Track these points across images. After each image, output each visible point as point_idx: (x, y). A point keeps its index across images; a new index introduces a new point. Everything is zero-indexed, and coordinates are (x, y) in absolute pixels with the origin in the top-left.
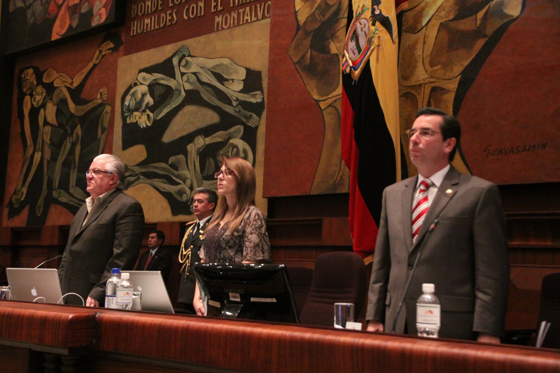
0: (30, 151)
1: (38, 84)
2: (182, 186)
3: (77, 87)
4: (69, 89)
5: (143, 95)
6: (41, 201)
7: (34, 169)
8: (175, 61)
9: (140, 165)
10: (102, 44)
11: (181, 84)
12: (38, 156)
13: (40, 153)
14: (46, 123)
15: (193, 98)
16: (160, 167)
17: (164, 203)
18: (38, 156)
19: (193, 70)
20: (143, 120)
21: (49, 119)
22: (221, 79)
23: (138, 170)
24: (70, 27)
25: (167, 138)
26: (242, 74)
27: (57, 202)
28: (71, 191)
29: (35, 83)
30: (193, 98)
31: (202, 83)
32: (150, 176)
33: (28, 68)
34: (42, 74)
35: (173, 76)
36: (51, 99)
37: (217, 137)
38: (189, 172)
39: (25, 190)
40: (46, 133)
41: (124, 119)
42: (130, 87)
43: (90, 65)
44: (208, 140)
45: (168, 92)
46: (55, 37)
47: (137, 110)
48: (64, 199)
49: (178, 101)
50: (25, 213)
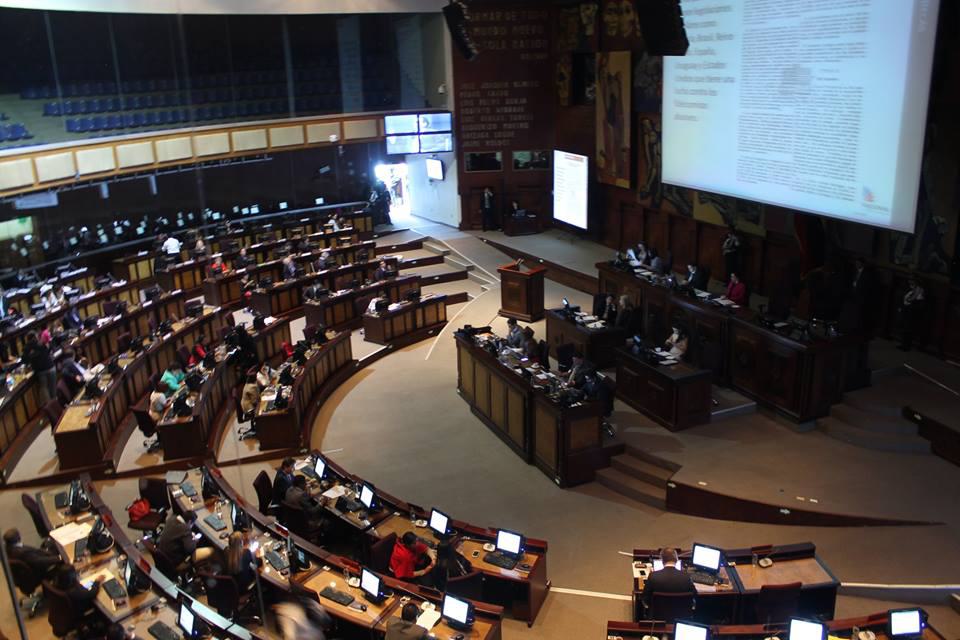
0: (650, 166)
6: (658, 195)
7: (653, 177)
17: (720, 217)
27: (666, 198)
39: (648, 187)
48: (670, 198)
50: (650, 199)
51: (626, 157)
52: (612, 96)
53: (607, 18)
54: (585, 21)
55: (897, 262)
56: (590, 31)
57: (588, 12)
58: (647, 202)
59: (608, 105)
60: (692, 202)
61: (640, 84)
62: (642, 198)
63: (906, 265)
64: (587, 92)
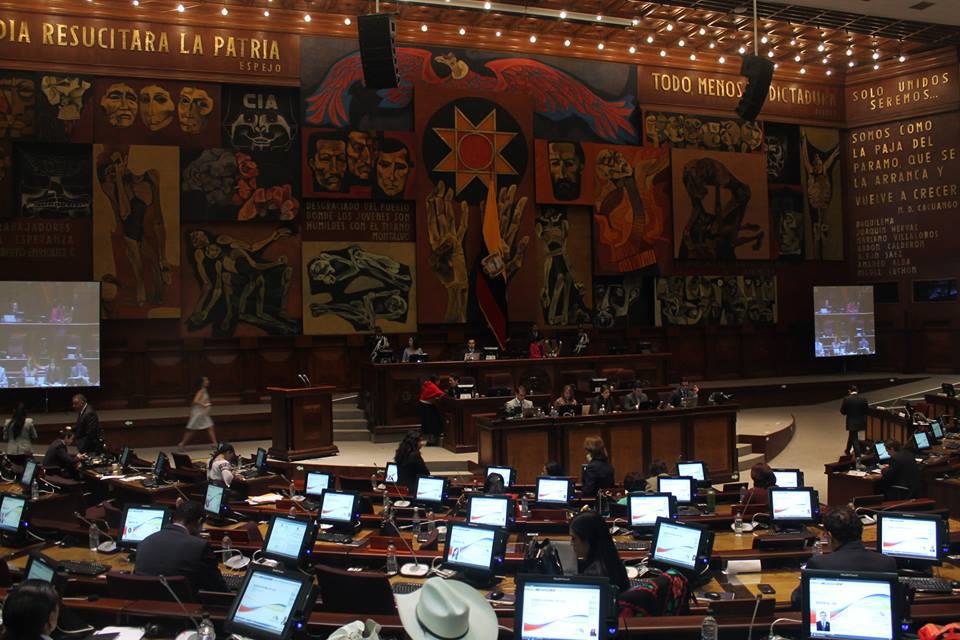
1: (211, 244)
2: (362, 316)
3: (256, 252)
4: (248, 252)
5: (326, 266)
8: (350, 251)
9: (329, 304)
10: (281, 227)
11: (356, 263)
12: (218, 292)
13: (220, 291)
14: (224, 270)
15: (364, 272)
16: (345, 306)
17: (349, 324)
18: (218, 292)
19: (365, 258)
20: (328, 280)
21: (228, 268)
22: (385, 267)
23: (326, 307)
24: (258, 215)
25: (347, 291)
26: (398, 266)
28: (259, 315)
29: (208, 241)
30: (364, 272)
31: (372, 267)
32: (336, 310)
33: (198, 230)
34: (217, 236)
35: (349, 259)
36: (229, 256)
37: (384, 294)
38: (366, 311)
39: (206, 313)
40: (227, 278)
41: (311, 278)
42: (314, 261)
43: (269, 240)
44: (377, 295)
45: (346, 268)
46: (241, 218)
47: (322, 273)
48: (252, 320)
49: (356, 272)
51: (168, 278)
52: (135, 202)
53: (106, 102)
54: (54, 100)
55: (551, 322)
56: (69, 114)
57: (60, 88)
58: (207, 332)
59: (125, 213)
60: (300, 321)
61: (196, 188)
62: (192, 326)
63: (560, 323)
64: (24, 202)
